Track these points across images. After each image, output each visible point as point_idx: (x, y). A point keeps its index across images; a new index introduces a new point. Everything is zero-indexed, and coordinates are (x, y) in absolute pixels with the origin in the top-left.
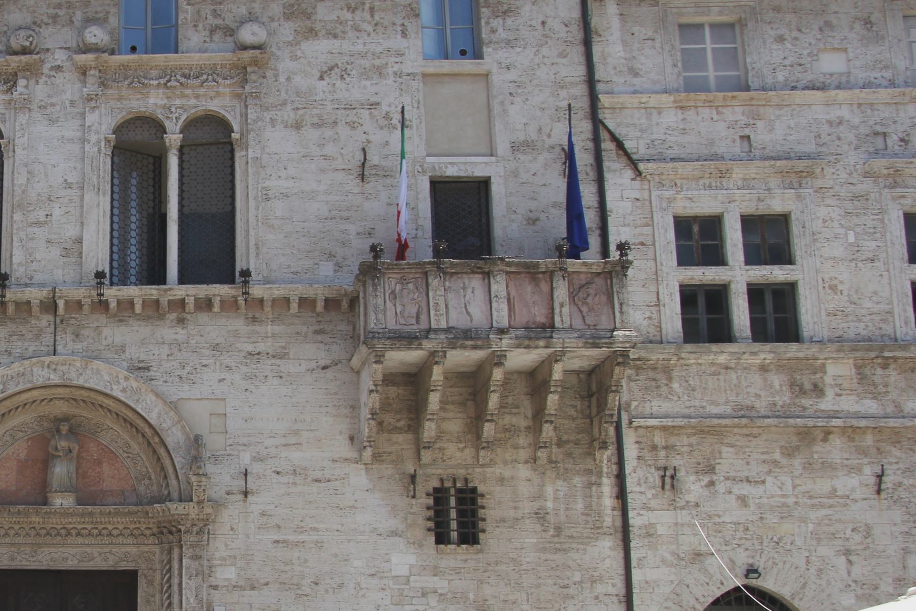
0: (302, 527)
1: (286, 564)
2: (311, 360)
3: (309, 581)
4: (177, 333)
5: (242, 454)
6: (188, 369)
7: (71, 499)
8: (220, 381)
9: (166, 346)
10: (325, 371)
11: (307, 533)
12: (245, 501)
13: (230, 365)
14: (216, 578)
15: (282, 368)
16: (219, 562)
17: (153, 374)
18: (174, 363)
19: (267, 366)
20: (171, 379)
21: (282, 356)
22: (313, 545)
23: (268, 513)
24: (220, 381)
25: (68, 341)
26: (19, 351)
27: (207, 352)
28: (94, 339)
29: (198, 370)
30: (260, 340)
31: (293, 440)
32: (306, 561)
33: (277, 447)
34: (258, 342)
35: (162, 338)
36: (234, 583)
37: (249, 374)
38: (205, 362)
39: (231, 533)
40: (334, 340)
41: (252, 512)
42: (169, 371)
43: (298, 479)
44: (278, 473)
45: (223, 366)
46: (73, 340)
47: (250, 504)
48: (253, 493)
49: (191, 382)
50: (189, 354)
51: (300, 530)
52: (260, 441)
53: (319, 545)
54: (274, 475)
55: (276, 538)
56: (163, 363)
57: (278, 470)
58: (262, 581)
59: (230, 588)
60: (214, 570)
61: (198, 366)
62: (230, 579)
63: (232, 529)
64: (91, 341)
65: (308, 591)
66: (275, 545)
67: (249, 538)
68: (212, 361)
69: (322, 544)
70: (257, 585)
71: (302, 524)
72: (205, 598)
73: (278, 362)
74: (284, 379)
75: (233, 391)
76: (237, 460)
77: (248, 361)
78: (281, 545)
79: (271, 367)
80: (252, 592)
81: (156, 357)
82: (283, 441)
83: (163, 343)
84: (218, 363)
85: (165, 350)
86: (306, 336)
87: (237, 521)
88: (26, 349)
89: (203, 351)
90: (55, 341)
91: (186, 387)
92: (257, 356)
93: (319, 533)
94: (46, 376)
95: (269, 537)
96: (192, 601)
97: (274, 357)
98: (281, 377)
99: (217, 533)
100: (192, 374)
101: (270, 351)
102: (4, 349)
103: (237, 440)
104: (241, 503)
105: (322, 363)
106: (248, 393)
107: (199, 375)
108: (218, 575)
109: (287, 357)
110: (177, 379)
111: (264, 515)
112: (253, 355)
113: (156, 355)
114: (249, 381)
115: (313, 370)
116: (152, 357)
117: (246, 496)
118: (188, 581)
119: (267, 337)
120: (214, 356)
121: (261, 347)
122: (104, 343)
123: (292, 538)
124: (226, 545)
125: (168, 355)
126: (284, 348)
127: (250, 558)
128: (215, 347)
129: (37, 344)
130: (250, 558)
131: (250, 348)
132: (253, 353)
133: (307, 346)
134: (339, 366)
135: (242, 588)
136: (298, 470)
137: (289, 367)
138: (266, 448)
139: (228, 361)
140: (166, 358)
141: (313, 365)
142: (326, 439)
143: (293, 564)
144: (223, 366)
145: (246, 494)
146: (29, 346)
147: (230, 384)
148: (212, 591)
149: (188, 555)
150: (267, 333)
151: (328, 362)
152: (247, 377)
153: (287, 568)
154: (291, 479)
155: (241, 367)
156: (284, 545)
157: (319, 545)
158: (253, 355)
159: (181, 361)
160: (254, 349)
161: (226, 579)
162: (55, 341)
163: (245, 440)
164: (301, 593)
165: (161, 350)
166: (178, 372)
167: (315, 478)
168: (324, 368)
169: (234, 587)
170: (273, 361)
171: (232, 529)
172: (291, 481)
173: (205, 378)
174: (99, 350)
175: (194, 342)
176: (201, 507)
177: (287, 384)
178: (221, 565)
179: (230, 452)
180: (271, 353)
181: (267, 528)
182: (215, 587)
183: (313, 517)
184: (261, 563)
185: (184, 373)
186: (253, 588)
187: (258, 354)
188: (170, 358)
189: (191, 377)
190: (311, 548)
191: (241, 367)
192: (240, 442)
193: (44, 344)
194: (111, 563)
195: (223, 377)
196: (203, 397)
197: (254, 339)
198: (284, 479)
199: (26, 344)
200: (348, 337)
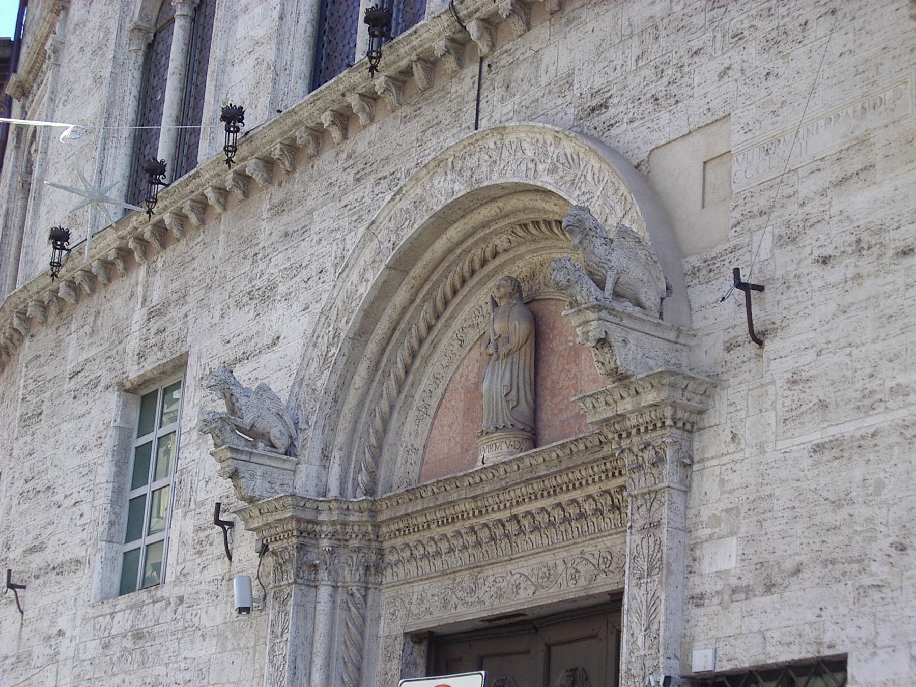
0: (872, 392)
1: (837, 505)
3: (885, 543)
7: (504, 446)
8: (721, 75)
11: (881, 408)
12: (759, 356)
16: (708, 531)
23: (805, 375)
24: (721, 75)
32: (880, 485)
36: (734, 581)
37: (774, 34)
38: (696, 44)
39: (732, 448)
41: (773, 382)
43: (866, 264)
54: (817, 269)
55: (817, 437)
57: (825, 252)
58: (789, 565)
62: (727, 572)
66: (816, 457)
71: (874, 384)
75: (744, 89)
78: (828, 455)
82: (836, 173)
95: (804, 439)
99: (707, 455)
111: (794, 382)
123: (849, 428)
127: (765, 505)
130: (765, 505)
135: (748, 591)
136: (865, 237)
143: (852, 502)
149: (637, 526)
153: (842, 515)
156: (836, 452)
161: (719, 574)
163: (762, 202)
164: (866, 581)
167: (901, 245)
178: (711, 538)
182: (698, 600)
184: (787, 514)
186: (770, 588)
190: (891, 447)
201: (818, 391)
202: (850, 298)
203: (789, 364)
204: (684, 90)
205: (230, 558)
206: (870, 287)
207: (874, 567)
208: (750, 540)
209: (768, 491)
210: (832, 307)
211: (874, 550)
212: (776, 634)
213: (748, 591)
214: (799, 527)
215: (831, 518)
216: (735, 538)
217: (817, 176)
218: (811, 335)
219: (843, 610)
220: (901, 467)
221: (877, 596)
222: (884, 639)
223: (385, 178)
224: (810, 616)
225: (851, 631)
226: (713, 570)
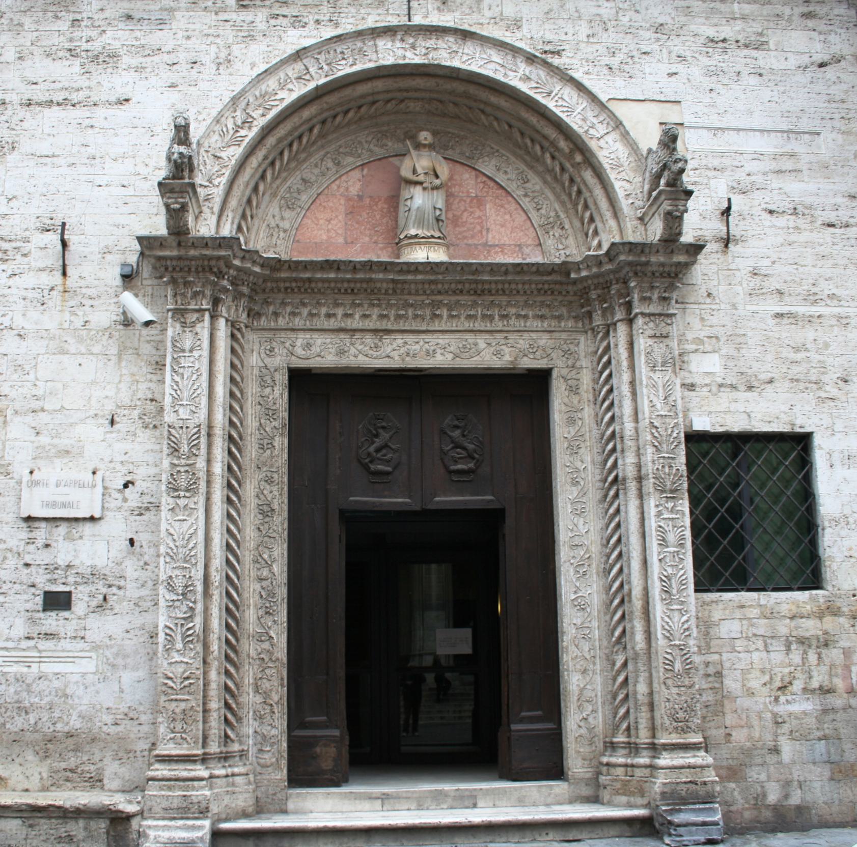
1: (797, 350)
2: (802, 53)
4: (599, 6)
5: (712, 182)
6: (620, 57)
8: (671, 75)
9: (584, 24)
10: (823, 69)
11: (823, 304)
13: (683, 54)
14: (690, 372)
15: (761, 63)
17: (567, 61)
18: (597, 47)
19: (738, 59)
20: (596, 69)
21: (761, 46)
22: (834, 322)
23: (763, 272)
24: (671, 75)
25: (430, 9)
26: (351, 20)
27: (649, 34)
28: (471, 8)
29: (636, 59)
30: (724, 22)
31: (788, 165)
32: (827, 345)
33: (765, 174)
34: (721, 25)
35: (577, 11)
36: (719, 380)
37: (714, 68)
40: (830, 28)
41: (739, 270)
42: (591, 57)
43: (801, 222)
44: (771, 212)
45: (674, 55)
46: (439, 9)
47: (734, 257)
48: (736, 241)
49: (628, 75)
50: (621, 35)
51: (813, 298)
52: (739, 164)
53: (844, 321)
54: (766, 215)
55: (778, 309)
56: (582, 46)
58: (764, 377)
59: (714, 389)
60: (686, 358)
61: (635, 53)
63: (709, 295)
64: (467, 11)
65: (834, 392)
66: (777, 320)
67: (736, 309)
68: (656, 47)
69: (848, 321)
70: (755, 384)
71: (814, 290)
72: (679, 402)
73: (754, 53)
74: (764, 77)
76: (707, 191)
77: (710, 50)
78: (785, 321)
79: (744, 61)
80: (749, 394)
81: (569, 37)
82: (774, 166)
83: (580, 18)
84: (664, 50)
85: (583, 30)
86: (790, 20)
87: (716, 283)
88: (363, 19)
89: (641, 32)
90: (409, 8)
91: (619, 82)
92: (721, 45)
93: (842, 303)
94: (400, 52)
96: (659, 406)
97: (747, 46)
98: (760, 75)
100: (626, 63)
101: (740, 38)
102: (327, 18)
103: (704, 162)
104: (719, 255)
105: (819, 58)
106: (714, 95)
107: (638, 66)
108: (693, 367)
109: (766, 47)
110: (605, 71)
111: (755, 274)
112: (717, 43)
113: (570, 34)
114: (714, 78)
115: (806, 67)
116: (564, 37)
117: (726, 246)
118: (651, 374)
119: (735, 19)
120: (658, 40)
121: (727, 31)
122: (488, 14)
123: (802, 310)
124: (702, 319)
125: (588, 36)
126: (761, 34)
128: (659, 28)
129: (380, 11)
131: (711, 32)
132: (716, 39)
133: (794, 34)
134: (843, 63)
136: (800, 209)
137: (767, 60)
138: (749, 175)
139: (679, 49)
140: (585, 40)
141: (806, 60)
142: (836, 165)
143: (807, 350)
144: (674, 55)
145: (727, 241)
146: (369, 14)
147: (686, 81)
148: (687, 393)
150: (733, 13)
151: (826, 58)
152: (711, 73)
153: (800, 356)
154: (791, 221)
155: (700, 57)
157: (844, 321)
158: (717, 43)
159: (610, 46)
160: (716, 35)
161: (707, 374)
162: (409, 8)
163: (716, 163)
164: (824, 395)
165: (577, 28)
166: (606, 60)
167: (827, 221)
168: (821, 65)
169: (721, 386)
170: (746, 52)
171: (709, 295)
172: (791, 224)
173: (647, 70)
174: (482, 24)
175: (627, 19)
176: (669, 250)
177: (770, 84)
179: (696, 179)
180: (742, 41)
181: (763, 294)
182: (691, 387)
183: (830, 279)
184: (759, 347)
185: (615, 62)
186: (750, 388)
187: (724, 41)
188: (591, 40)
189: (627, 68)
190: (832, 326)
191: (700, 57)
192: (710, 166)
193: (391, 11)
194: (507, 358)
195: (674, 70)
196: (647, 97)
197: (715, 21)
198: (782, 221)
199: (363, 11)
200: (851, 25)
201: (774, 284)
202: (793, 238)
203: (751, 263)
204: (637, 72)
205: (64, 274)
206: (805, 236)
207: (827, 388)
208: (729, 357)
209: (742, 332)
210: (780, 240)
211: (825, 378)
212: (759, 416)
213: (733, 387)
214: (769, 357)
215: (793, 356)
216: (717, 355)
217: (756, 163)
218: (766, 250)
219: (807, 408)
220: (841, 339)
221: (831, 404)
222: (839, 426)
223: (284, 16)
224: (785, 408)
225: (815, 420)
226: (701, 370)
